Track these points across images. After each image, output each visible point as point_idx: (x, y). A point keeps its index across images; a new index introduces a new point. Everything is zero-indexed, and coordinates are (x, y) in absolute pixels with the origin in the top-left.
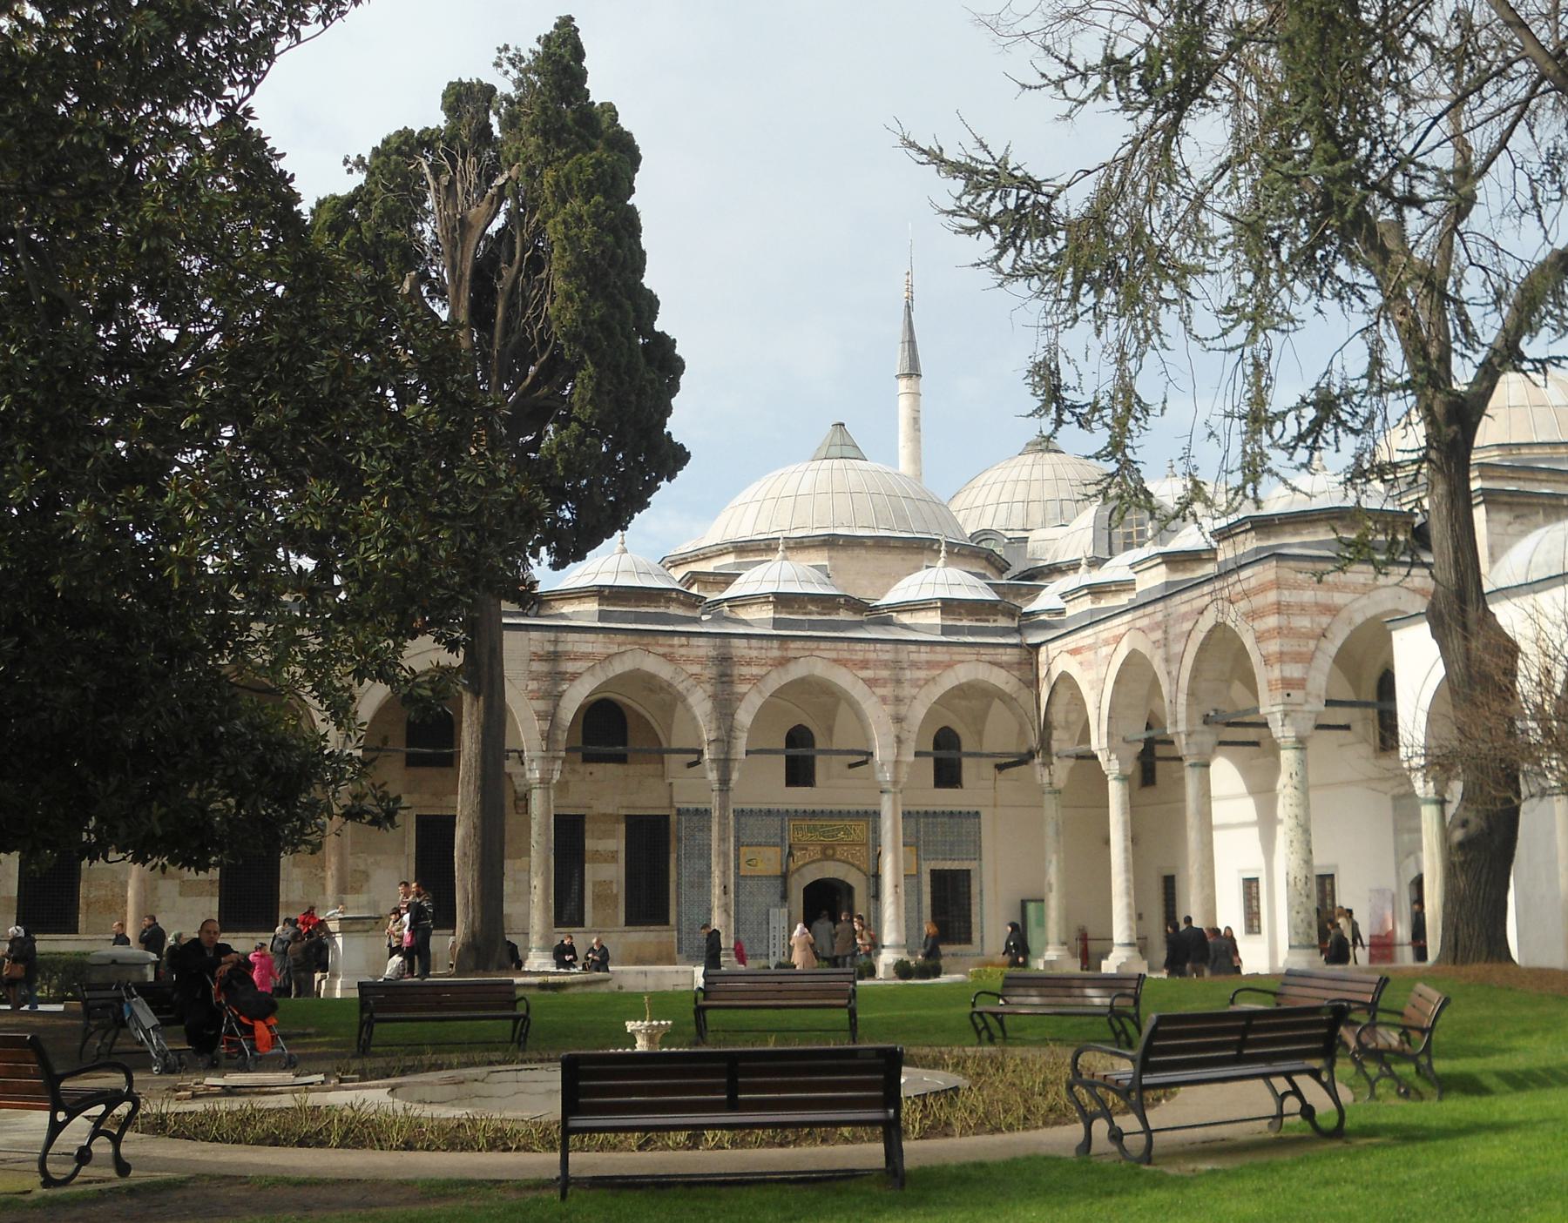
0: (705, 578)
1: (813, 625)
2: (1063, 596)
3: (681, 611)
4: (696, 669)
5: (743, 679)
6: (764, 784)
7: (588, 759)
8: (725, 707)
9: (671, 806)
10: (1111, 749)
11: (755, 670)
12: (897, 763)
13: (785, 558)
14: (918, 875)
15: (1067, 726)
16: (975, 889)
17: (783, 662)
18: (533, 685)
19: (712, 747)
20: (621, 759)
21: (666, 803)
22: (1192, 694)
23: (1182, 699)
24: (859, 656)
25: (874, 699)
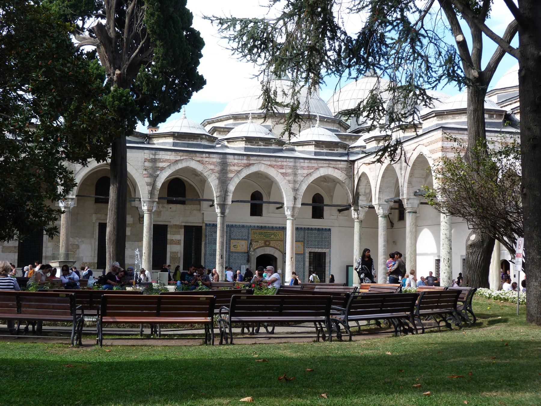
0: (219, 129)
1: (260, 150)
2: (365, 141)
3: (206, 143)
4: (212, 167)
5: (232, 172)
6: (242, 215)
7: (169, 202)
8: (224, 182)
9: (203, 223)
10: (380, 205)
11: (236, 168)
12: (294, 208)
13: (252, 122)
14: (304, 254)
15: (365, 195)
16: (327, 260)
17: (248, 165)
18: (145, 172)
19: (218, 199)
20: (183, 203)
21: (201, 221)
22: (410, 183)
23: (406, 185)
24: (279, 164)
25: (285, 181)
